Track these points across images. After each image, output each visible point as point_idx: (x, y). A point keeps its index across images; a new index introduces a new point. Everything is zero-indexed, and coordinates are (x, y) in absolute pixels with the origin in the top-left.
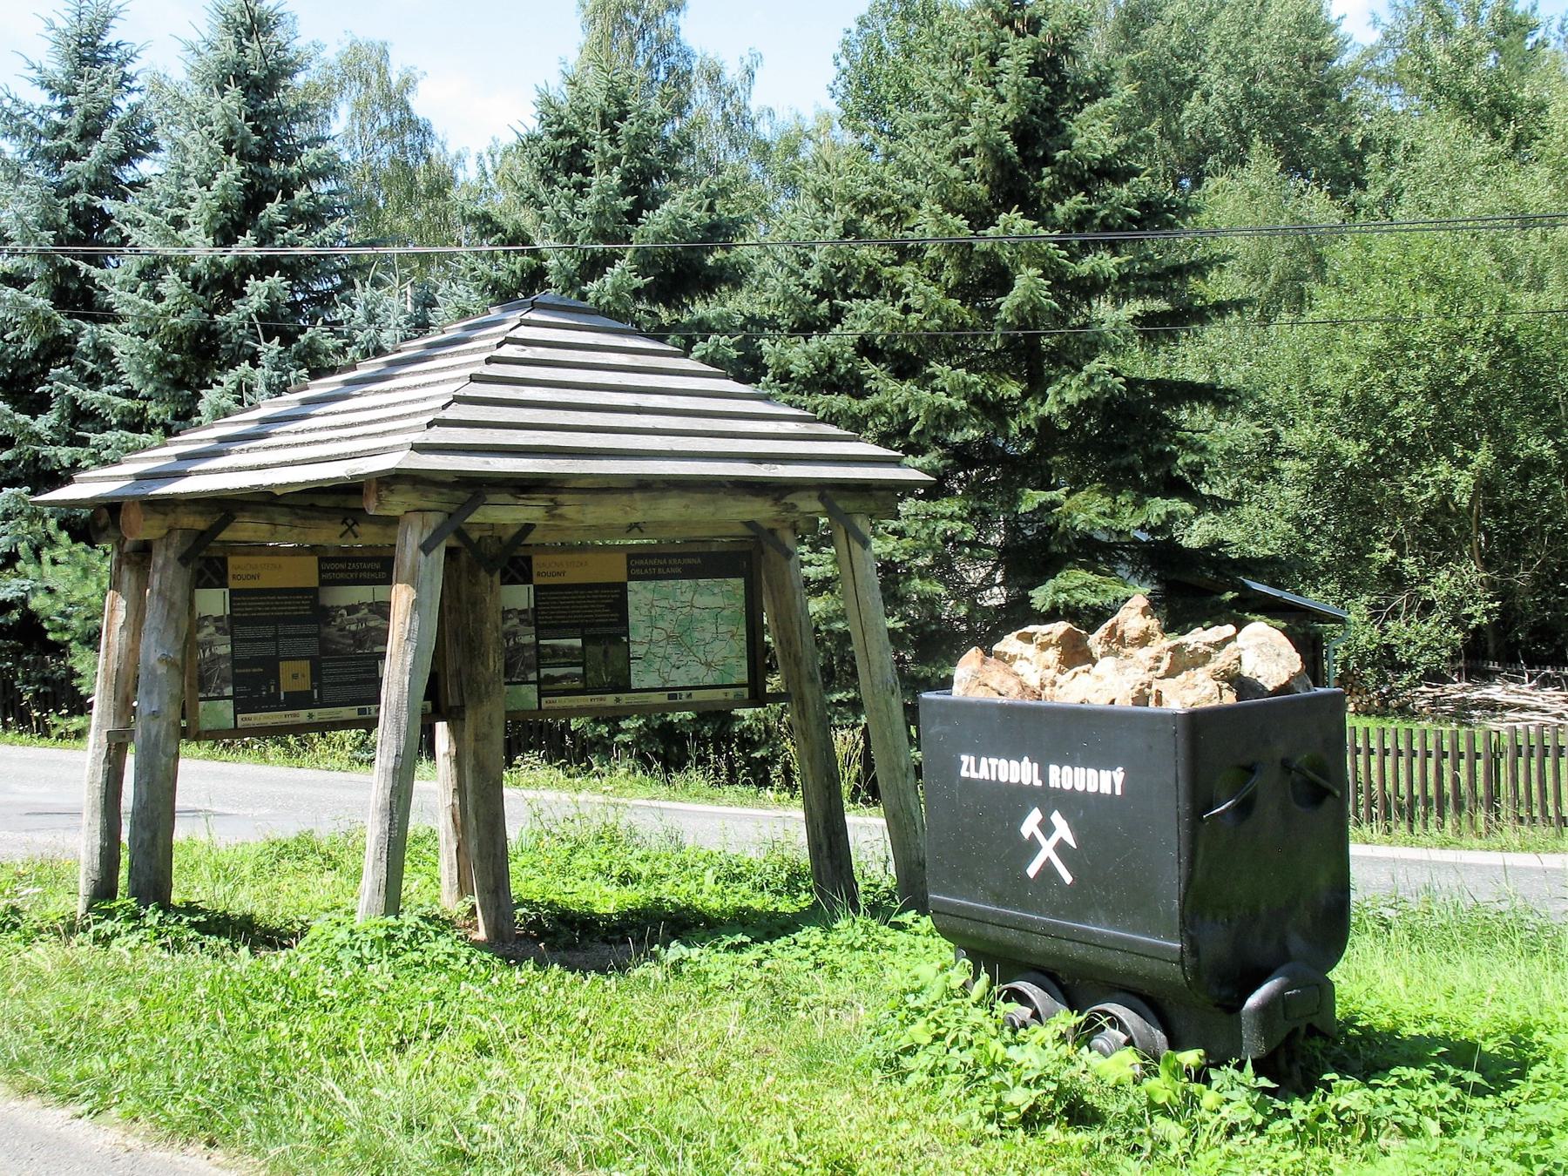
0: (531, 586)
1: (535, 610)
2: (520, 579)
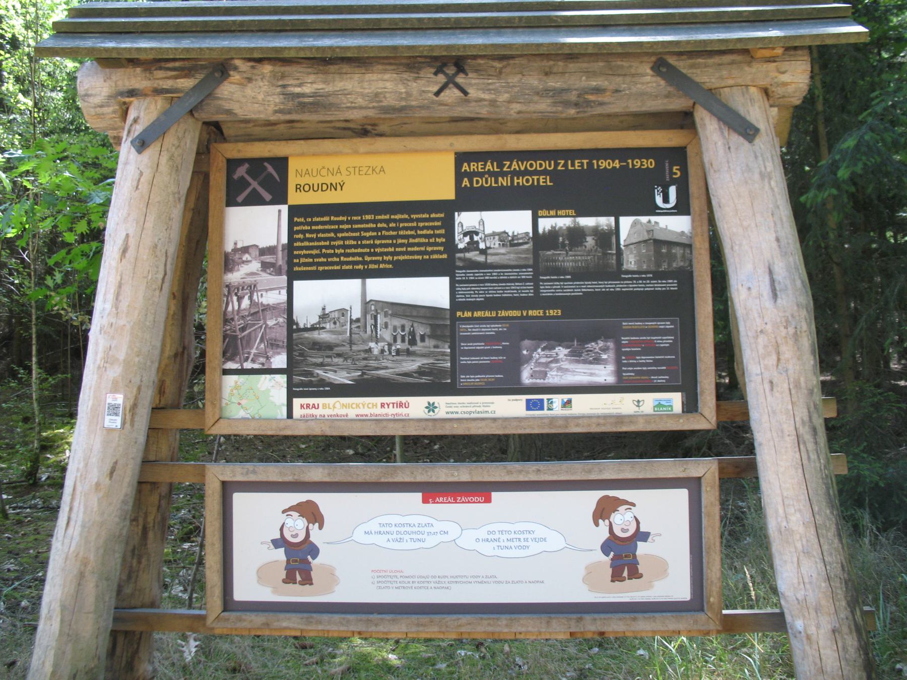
0: (284, 209)
1: (290, 247)
2: (268, 197)
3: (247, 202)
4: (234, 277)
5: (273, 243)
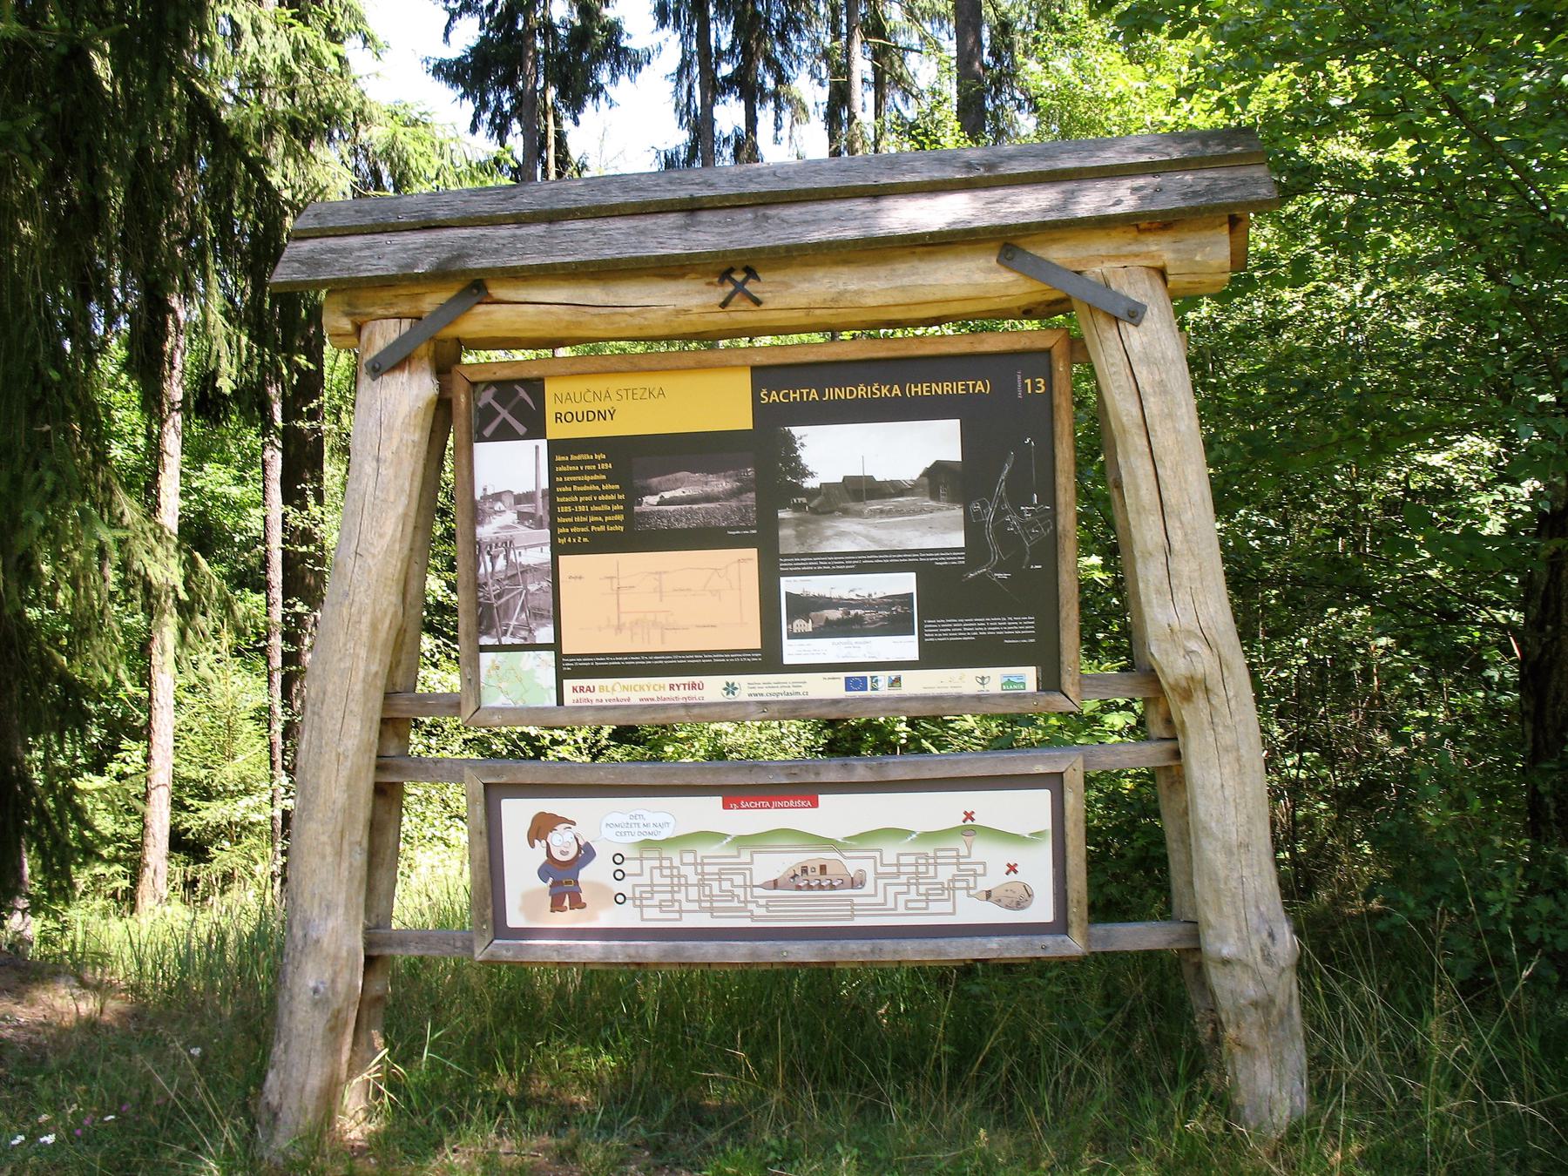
0: (543, 444)
1: (552, 493)
2: (521, 429)
3: (496, 437)
4: (485, 532)
5: (532, 488)
